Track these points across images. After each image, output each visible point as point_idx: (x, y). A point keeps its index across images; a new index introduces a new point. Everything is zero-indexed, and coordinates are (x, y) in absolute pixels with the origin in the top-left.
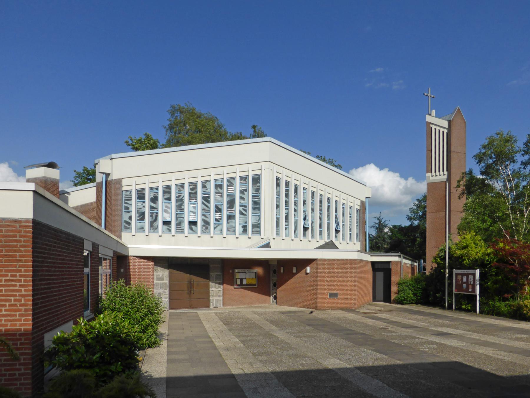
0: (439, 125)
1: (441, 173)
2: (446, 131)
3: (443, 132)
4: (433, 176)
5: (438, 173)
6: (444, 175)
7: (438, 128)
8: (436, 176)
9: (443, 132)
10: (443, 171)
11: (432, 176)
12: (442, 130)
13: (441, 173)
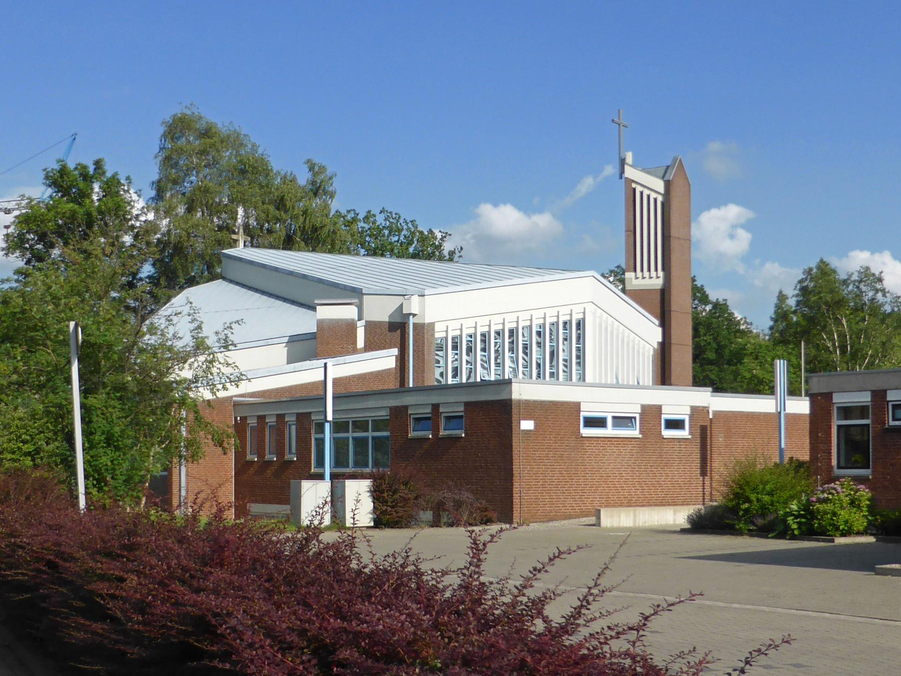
0: (649, 186)
1: (653, 274)
2: (660, 199)
3: (655, 200)
4: (638, 278)
5: (646, 274)
6: (658, 277)
7: (646, 192)
8: (644, 278)
9: (655, 200)
10: (656, 270)
11: (637, 278)
12: (653, 195)
13: (653, 274)
